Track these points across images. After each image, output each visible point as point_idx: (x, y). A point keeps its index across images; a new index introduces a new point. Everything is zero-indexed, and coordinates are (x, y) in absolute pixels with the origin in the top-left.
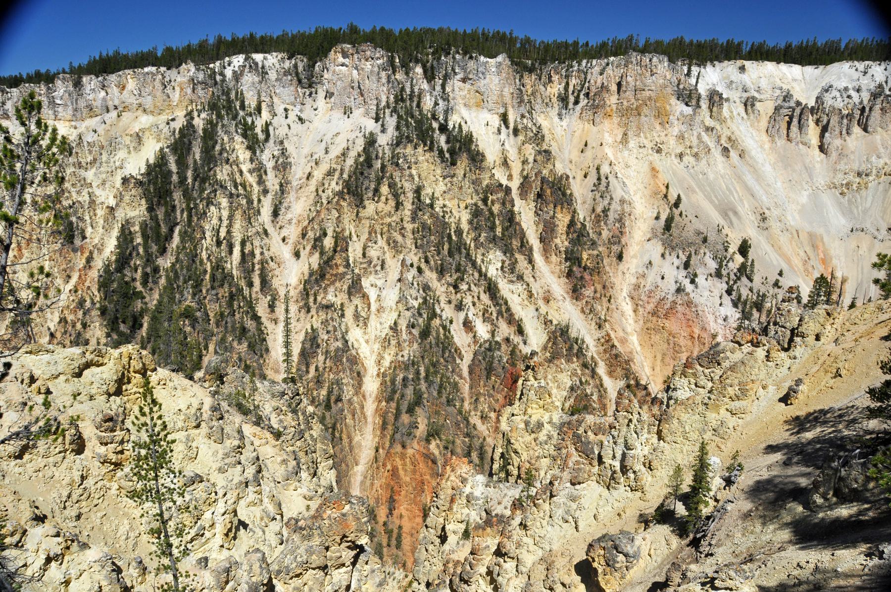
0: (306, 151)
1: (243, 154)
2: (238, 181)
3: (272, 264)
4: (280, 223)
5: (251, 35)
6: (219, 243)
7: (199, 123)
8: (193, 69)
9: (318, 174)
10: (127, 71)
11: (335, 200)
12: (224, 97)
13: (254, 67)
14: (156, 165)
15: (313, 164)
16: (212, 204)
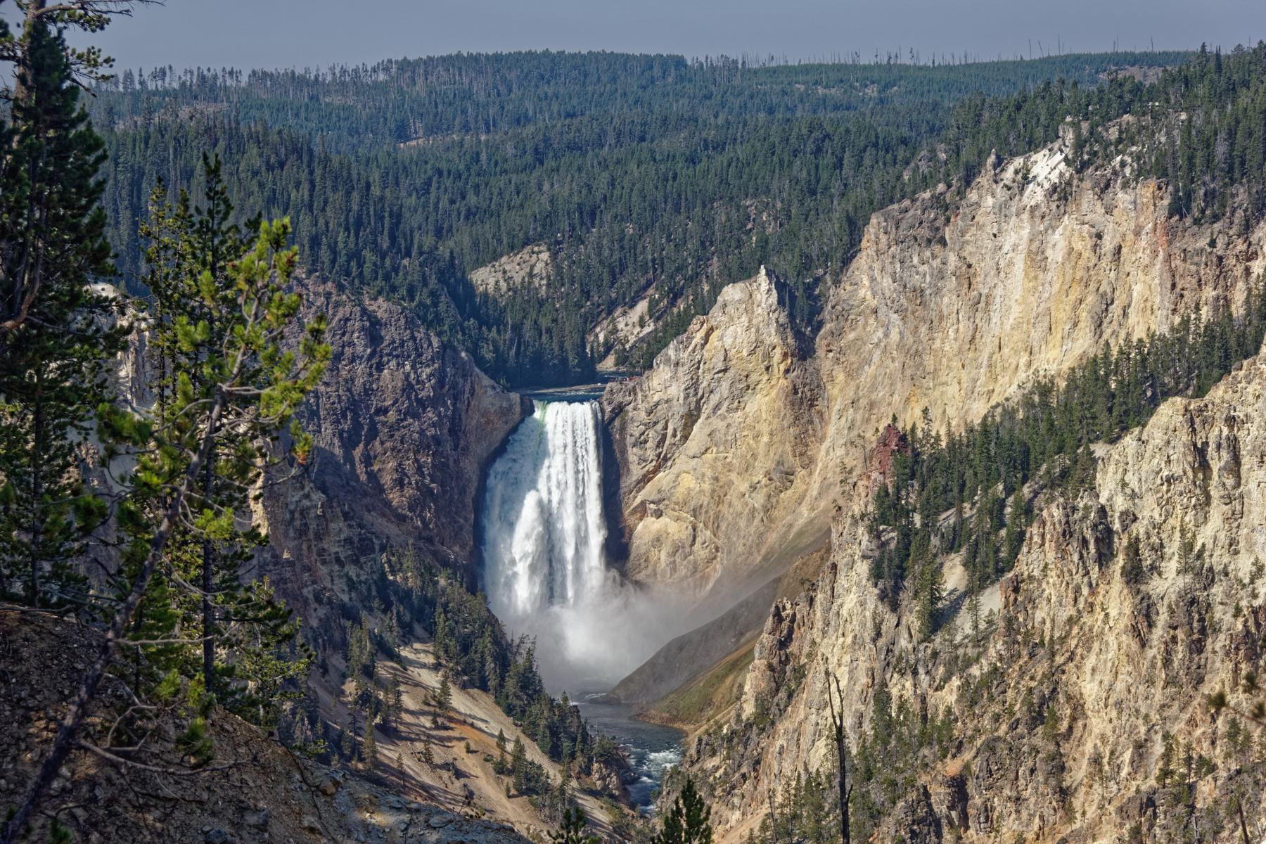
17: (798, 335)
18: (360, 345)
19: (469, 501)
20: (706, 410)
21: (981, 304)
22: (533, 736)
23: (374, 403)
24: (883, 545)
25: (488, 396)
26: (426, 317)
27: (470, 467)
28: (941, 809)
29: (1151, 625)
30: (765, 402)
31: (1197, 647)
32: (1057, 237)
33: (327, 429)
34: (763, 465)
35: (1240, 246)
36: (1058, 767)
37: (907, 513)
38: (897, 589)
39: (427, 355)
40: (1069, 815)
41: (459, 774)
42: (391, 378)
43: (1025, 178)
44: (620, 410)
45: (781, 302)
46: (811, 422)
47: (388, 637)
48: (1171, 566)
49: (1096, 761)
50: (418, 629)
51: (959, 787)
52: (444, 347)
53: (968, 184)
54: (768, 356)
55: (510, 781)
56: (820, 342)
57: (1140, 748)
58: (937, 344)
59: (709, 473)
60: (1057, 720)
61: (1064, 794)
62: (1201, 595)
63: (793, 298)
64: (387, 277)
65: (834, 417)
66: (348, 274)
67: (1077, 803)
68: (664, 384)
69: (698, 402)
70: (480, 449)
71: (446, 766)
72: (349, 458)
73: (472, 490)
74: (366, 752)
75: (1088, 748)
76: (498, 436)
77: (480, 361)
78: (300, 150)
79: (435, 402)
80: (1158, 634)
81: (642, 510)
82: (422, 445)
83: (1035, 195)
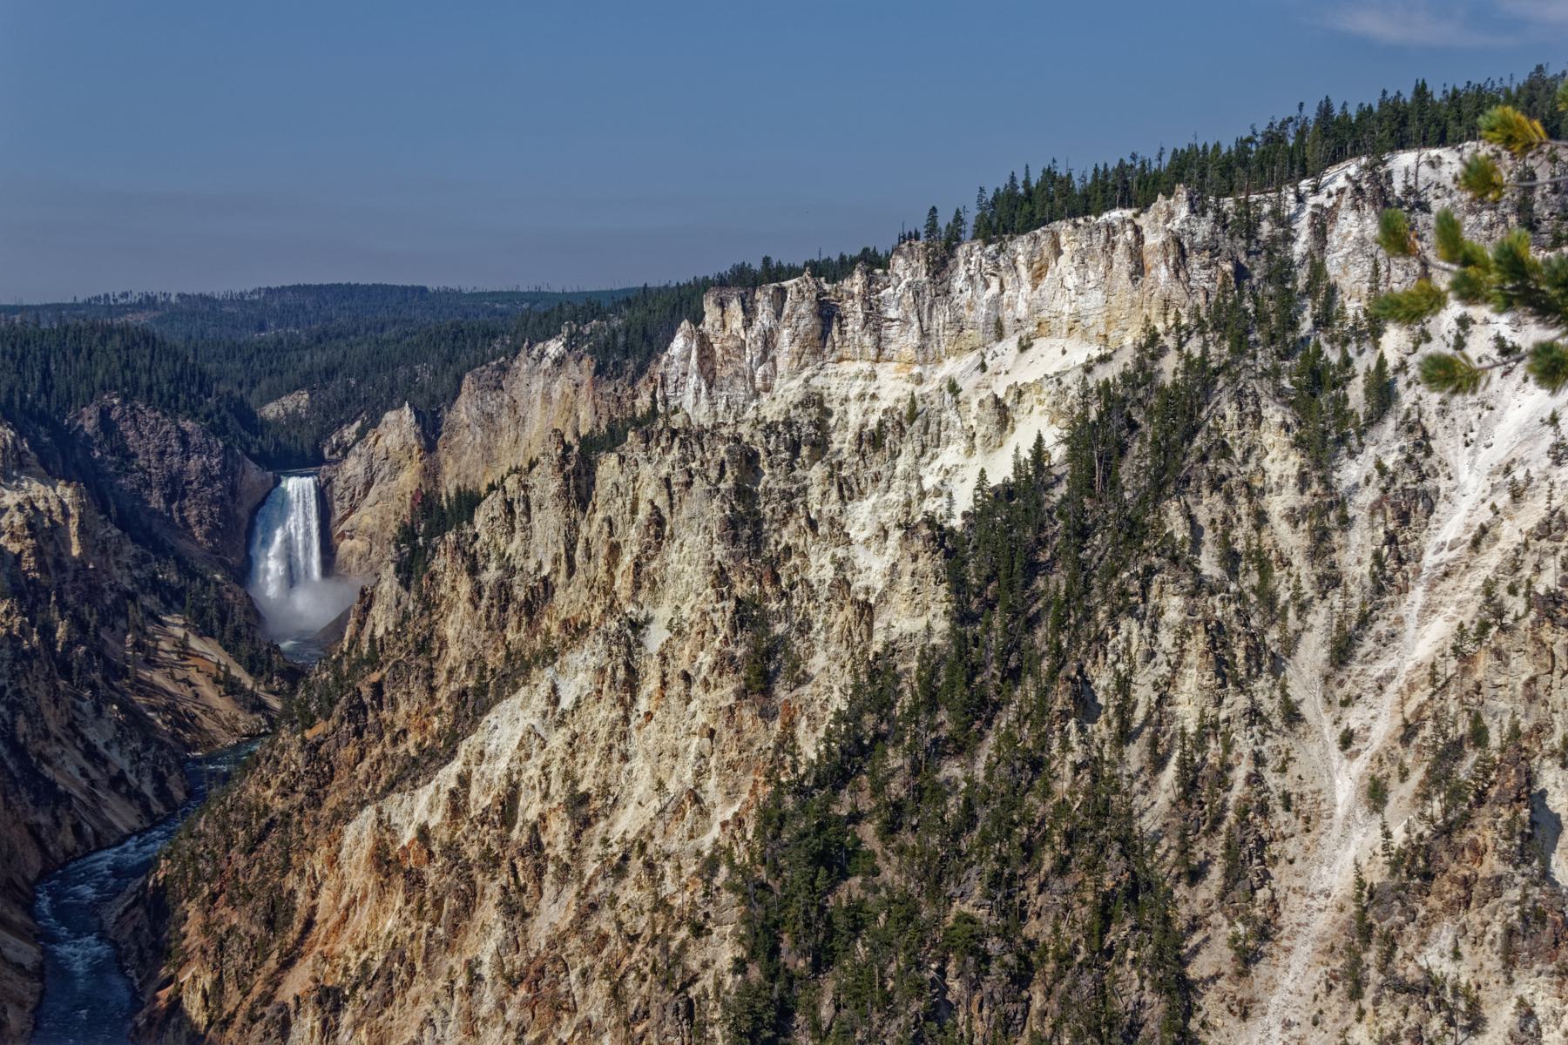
0: (1498, 454)
1: (1280, 461)
2: (1239, 547)
3: (1281, 816)
4: (1348, 685)
5: (1421, 91)
6: (1125, 736)
7: (1169, 368)
8: (1183, 211)
9: (1510, 534)
10: (1064, 228)
11: (1527, 622)
12: (1271, 289)
13: (1374, 192)
14: (1007, 493)
15: (1503, 500)
16: (1132, 611)
17: (427, 439)
18: (176, 447)
19: (242, 531)
20: (377, 480)
21: (520, 422)
22: (239, 662)
24: (402, 555)
25: (254, 474)
26: (219, 430)
27: (243, 513)
28: (367, 700)
29: (481, 598)
31: (504, 609)
32: (557, 385)
33: (156, 493)
35: (630, 392)
36: (431, 675)
37: (417, 537)
38: (409, 579)
39: (216, 451)
40: (432, 699)
41: (191, 684)
42: (194, 464)
43: (542, 354)
44: (329, 481)
47: (155, 609)
48: (493, 566)
49: (451, 672)
50: (176, 605)
51: (378, 689)
52: (226, 447)
53: (516, 355)
54: (410, 451)
55: (221, 687)
56: (440, 443)
57: (470, 663)
60: (431, 650)
61: (432, 690)
62: (507, 581)
63: (424, 419)
64: (192, 409)
66: (169, 406)
67: (438, 695)
70: (249, 504)
71: (184, 680)
72: (169, 509)
73: (245, 526)
74: (131, 673)
75: (447, 665)
76: (259, 497)
77: (248, 454)
78: (148, 339)
79: (220, 477)
80: (484, 602)
81: (342, 536)
82: (213, 502)
83: (547, 363)
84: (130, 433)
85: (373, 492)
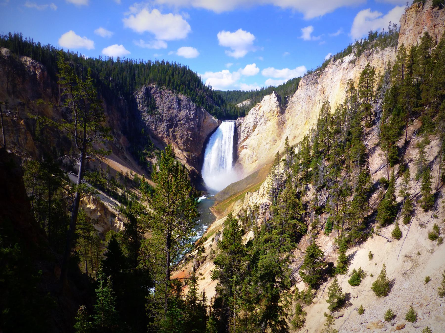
17: (281, 108)
23: (178, 119)
30: (272, 123)
33: (164, 124)
34: (270, 138)
39: (192, 108)
42: (183, 113)
44: (240, 124)
45: (278, 100)
46: (282, 129)
52: (197, 107)
54: (273, 113)
58: (314, 109)
59: (257, 140)
65: (288, 128)
68: (249, 119)
69: (257, 123)
84: (158, 99)
85: (257, 130)
